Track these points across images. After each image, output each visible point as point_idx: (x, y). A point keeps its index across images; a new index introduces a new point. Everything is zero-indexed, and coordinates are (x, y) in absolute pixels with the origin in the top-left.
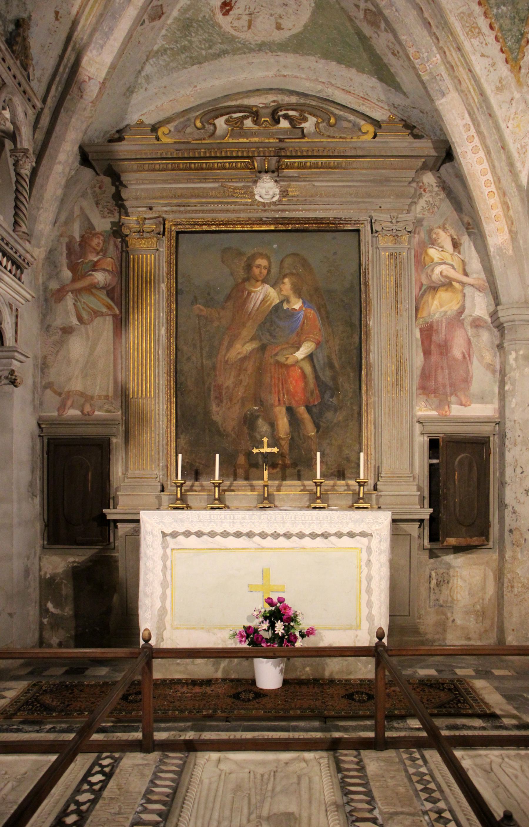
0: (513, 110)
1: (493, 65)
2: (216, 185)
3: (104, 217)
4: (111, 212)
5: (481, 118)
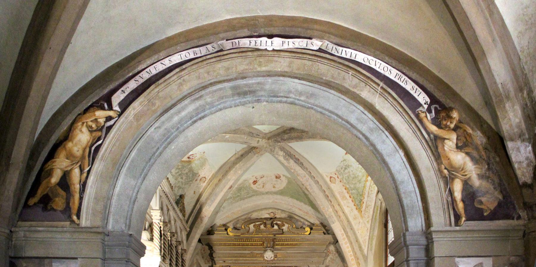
0: (360, 226)
1: (352, 210)
2: (249, 252)
3: (206, 264)
4: (208, 261)
5: (348, 230)
